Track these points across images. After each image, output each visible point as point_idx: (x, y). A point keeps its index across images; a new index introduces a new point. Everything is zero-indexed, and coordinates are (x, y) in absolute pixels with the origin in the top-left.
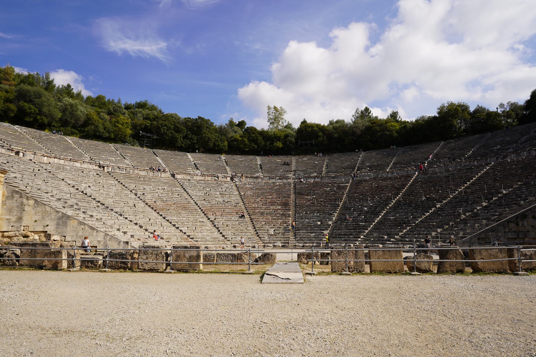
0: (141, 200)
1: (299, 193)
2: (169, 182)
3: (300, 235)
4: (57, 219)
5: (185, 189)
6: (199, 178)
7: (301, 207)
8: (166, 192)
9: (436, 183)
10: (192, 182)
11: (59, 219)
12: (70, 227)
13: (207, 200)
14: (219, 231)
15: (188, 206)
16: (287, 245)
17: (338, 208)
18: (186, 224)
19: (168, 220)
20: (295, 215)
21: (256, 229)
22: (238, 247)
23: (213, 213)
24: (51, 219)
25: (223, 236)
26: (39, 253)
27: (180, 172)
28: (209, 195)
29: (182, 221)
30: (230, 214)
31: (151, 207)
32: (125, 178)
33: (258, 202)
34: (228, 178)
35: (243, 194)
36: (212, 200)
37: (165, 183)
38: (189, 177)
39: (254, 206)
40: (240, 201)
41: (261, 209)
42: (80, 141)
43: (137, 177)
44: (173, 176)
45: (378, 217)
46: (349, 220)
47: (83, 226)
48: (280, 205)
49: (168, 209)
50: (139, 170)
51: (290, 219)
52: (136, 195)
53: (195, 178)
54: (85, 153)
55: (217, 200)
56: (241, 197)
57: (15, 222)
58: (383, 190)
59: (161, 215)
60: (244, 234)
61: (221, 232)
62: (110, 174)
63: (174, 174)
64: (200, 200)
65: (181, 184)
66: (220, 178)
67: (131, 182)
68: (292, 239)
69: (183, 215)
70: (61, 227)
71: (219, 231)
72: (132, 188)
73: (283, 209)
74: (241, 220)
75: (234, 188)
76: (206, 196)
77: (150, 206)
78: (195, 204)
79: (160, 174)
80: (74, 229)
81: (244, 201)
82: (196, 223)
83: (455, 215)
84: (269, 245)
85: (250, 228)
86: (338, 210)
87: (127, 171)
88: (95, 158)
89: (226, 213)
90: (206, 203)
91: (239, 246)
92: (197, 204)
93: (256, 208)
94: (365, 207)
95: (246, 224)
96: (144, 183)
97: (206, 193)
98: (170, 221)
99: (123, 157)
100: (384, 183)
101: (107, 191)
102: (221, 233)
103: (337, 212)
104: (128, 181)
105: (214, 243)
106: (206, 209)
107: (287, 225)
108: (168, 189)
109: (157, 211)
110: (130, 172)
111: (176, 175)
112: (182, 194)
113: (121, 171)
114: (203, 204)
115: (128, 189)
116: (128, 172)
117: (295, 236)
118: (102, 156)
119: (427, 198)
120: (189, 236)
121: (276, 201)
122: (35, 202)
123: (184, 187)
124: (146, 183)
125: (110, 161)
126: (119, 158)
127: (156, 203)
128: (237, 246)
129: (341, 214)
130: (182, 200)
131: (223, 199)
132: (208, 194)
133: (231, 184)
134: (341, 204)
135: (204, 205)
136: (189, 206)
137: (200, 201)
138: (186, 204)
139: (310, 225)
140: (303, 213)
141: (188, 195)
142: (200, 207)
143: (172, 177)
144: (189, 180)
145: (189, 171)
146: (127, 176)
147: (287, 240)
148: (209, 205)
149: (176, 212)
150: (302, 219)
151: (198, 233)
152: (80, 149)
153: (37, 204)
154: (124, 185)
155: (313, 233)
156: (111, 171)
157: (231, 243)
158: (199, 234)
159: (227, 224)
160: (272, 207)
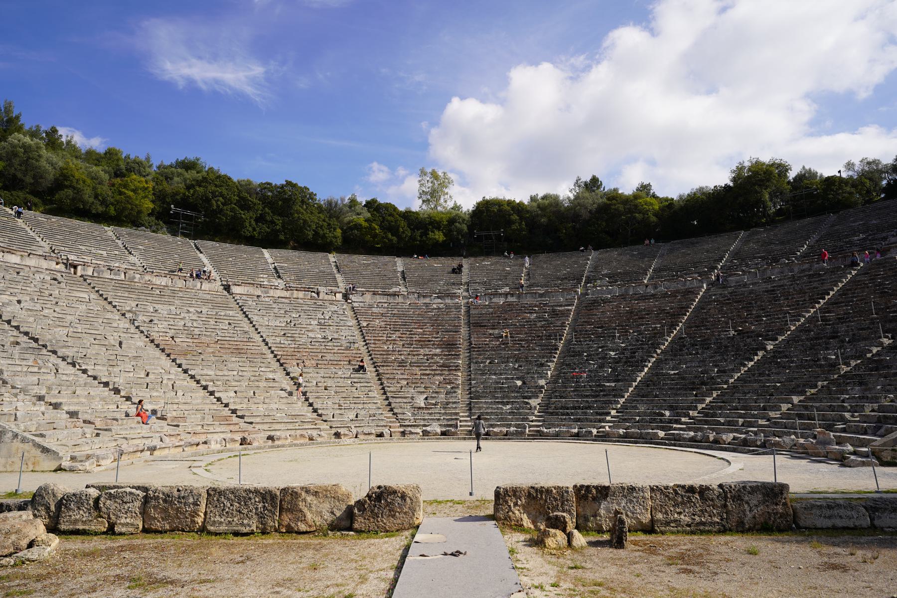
0: (142, 332)
1: (475, 324)
2: (215, 299)
3: (480, 408)
5: (247, 313)
6: (279, 293)
7: (481, 349)
8: (203, 319)
10: (264, 300)
13: (289, 335)
14: (307, 400)
15: (244, 347)
16: (453, 430)
17: (556, 353)
18: (234, 384)
19: (192, 377)
20: (470, 367)
21: (389, 394)
22: (345, 435)
23: (298, 361)
25: (315, 411)
27: (241, 281)
28: (295, 325)
29: (226, 378)
30: (335, 363)
31: (161, 347)
32: (119, 288)
33: (395, 340)
34: (337, 294)
35: (365, 324)
36: (301, 336)
37: (205, 302)
38: (258, 292)
39: (386, 347)
40: (358, 337)
41: (401, 355)
42: (40, 218)
43: (146, 288)
44: (227, 288)
45: (642, 371)
46: (581, 377)
48: (439, 346)
49: (200, 353)
50: (155, 274)
51: (460, 374)
52: (132, 321)
53: (272, 293)
54: (42, 240)
55: (311, 335)
56: (361, 331)
59: (180, 366)
60: (361, 406)
61: (311, 401)
62: (85, 280)
63: (229, 286)
64: (275, 334)
65: (240, 304)
66: (322, 296)
67: (130, 296)
68: (463, 417)
69: (230, 366)
71: (307, 400)
72: (128, 309)
73: (445, 355)
74: (357, 375)
75: (349, 313)
76: (289, 328)
77: (157, 346)
78: (263, 344)
79: (199, 284)
81: (366, 338)
82: (257, 383)
84: (413, 430)
85: (376, 393)
86: (557, 356)
87: (127, 277)
88: (63, 248)
89: (326, 362)
90: (286, 342)
91: (347, 432)
92: (267, 344)
93: (390, 353)
95: (366, 384)
96: (159, 299)
97: (291, 322)
98: (198, 378)
99: (128, 251)
101: (63, 312)
102: (311, 405)
103: (555, 360)
104: (123, 295)
105: (291, 426)
106: (285, 353)
107: (452, 388)
108: (209, 313)
109: (172, 357)
110: (134, 278)
111: (232, 287)
112: (239, 322)
113: (115, 274)
114: (280, 343)
115: (118, 310)
116: (129, 279)
117: (470, 409)
118: (80, 247)
119: (740, 333)
120: (234, 411)
121: (430, 339)
123: (245, 310)
124: (163, 299)
125: (95, 256)
126: (117, 253)
127: (175, 339)
128: (342, 433)
129: (563, 364)
130: (236, 335)
131: (323, 334)
132: (292, 324)
133: (343, 305)
134: (561, 345)
135: (282, 346)
136: (249, 347)
137: (274, 338)
138: (242, 344)
139: (501, 388)
140: (485, 362)
141: (252, 325)
142: (273, 349)
143: (224, 291)
144: (258, 296)
145: (262, 280)
146: (124, 286)
147: (452, 419)
148: (293, 346)
149: (217, 358)
150: (482, 374)
151: (257, 406)
152: (34, 231)
154: (110, 303)
155: (508, 403)
156: (91, 274)
157: (331, 427)
158: (260, 406)
159: (325, 384)
160: (422, 350)
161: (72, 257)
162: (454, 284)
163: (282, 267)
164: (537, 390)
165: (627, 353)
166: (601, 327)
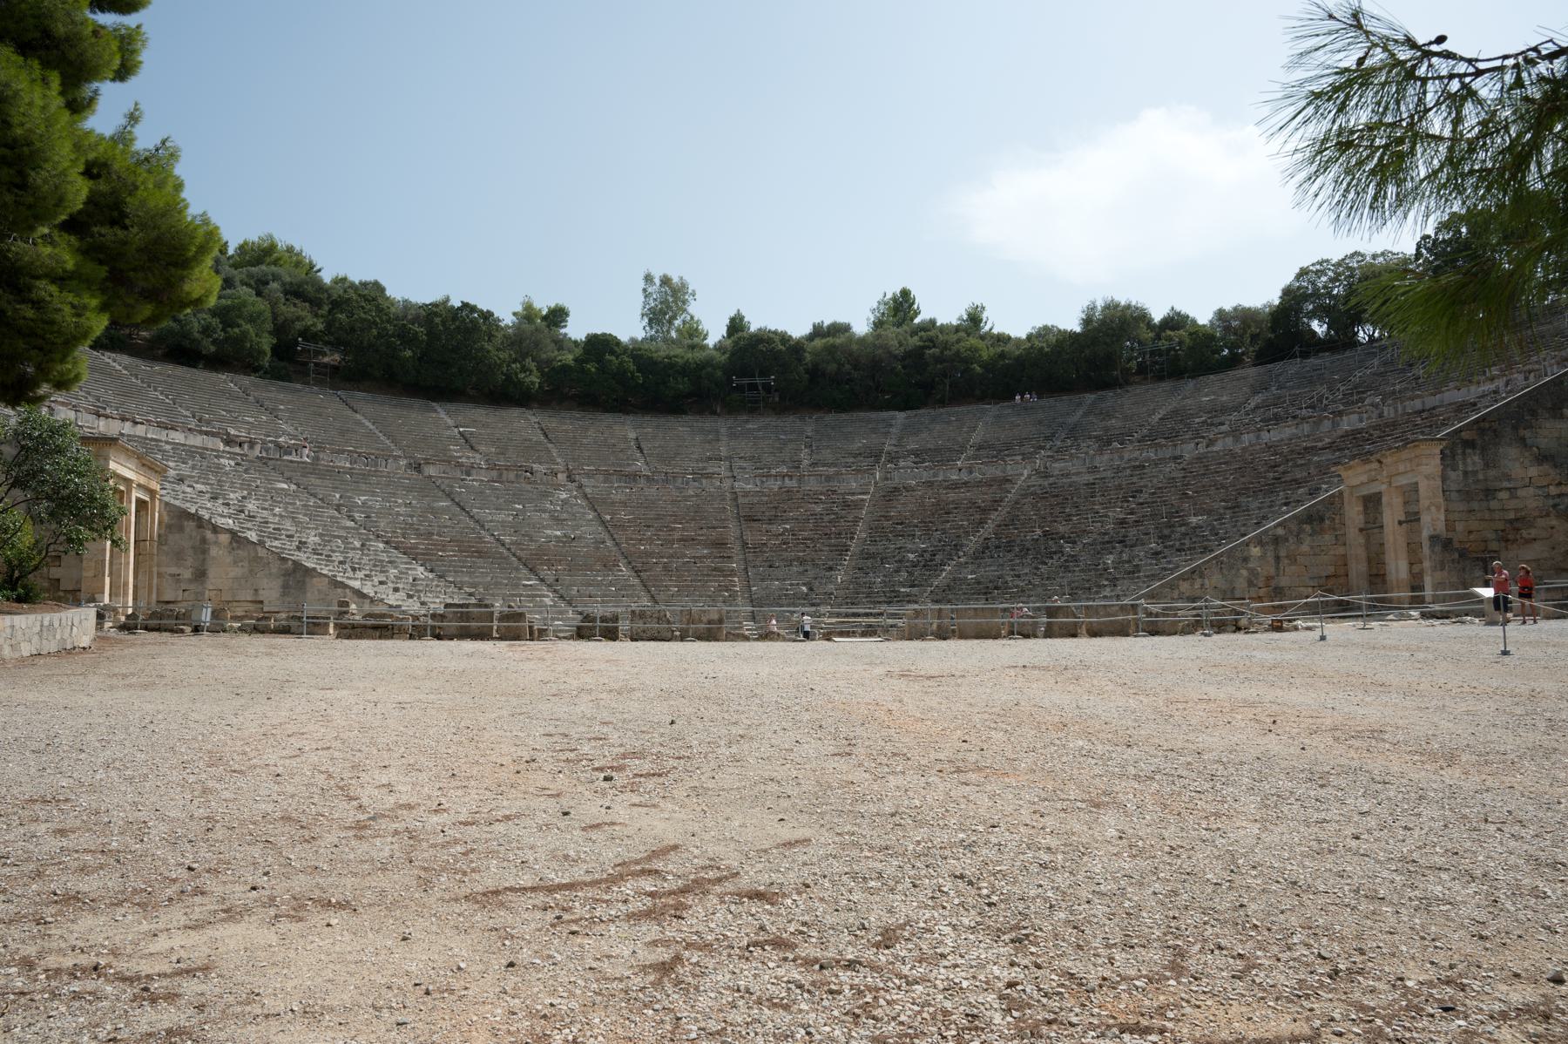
4: (284, 575)
9: (1067, 499)
11: (287, 574)
17: (847, 555)
24: (270, 574)
34: (559, 475)
35: (608, 517)
40: (607, 537)
47: (339, 590)
51: (736, 579)
57: (190, 581)
58: (949, 513)
70: (292, 591)
83: (1098, 570)
94: (908, 552)
100: (952, 496)
103: (846, 563)
119: (1045, 534)
139: (785, 595)
153: (237, 542)
162: (710, 459)
163: (472, 433)
164: (827, 597)
165: (927, 556)
166: (901, 524)
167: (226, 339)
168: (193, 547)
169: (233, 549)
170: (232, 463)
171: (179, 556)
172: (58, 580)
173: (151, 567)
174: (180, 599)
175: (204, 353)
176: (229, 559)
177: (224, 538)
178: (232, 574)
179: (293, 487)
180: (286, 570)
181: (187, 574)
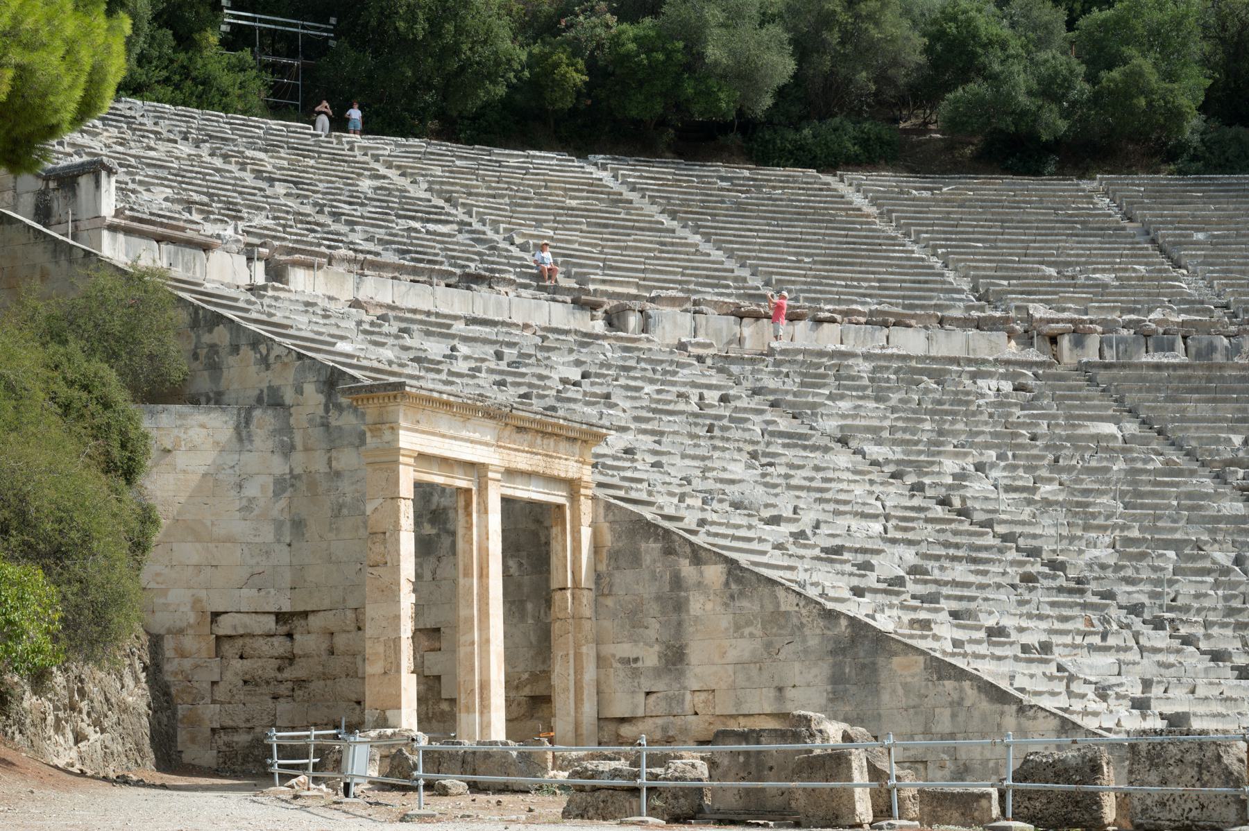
4: (833, 653)
12: (894, 691)
24: (806, 651)
26: (771, 768)
70: (853, 689)
80: (911, 703)
122: (729, 573)
152: (916, 242)
153: (739, 581)
161: (1039, 311)
167: (1096, 100)
168: (658, 598)
169: (732, 597)
170: (1007, 386)
171: (634, 618)
172: (438, 678)
173: (577, 646)
174: (640, 713)
175: (1044, 138)
176: (725, 621)
177: (714, 573)
178: (732, 655)
179: (1132, 427)
180: (837, 640)
181: (651, 657)
